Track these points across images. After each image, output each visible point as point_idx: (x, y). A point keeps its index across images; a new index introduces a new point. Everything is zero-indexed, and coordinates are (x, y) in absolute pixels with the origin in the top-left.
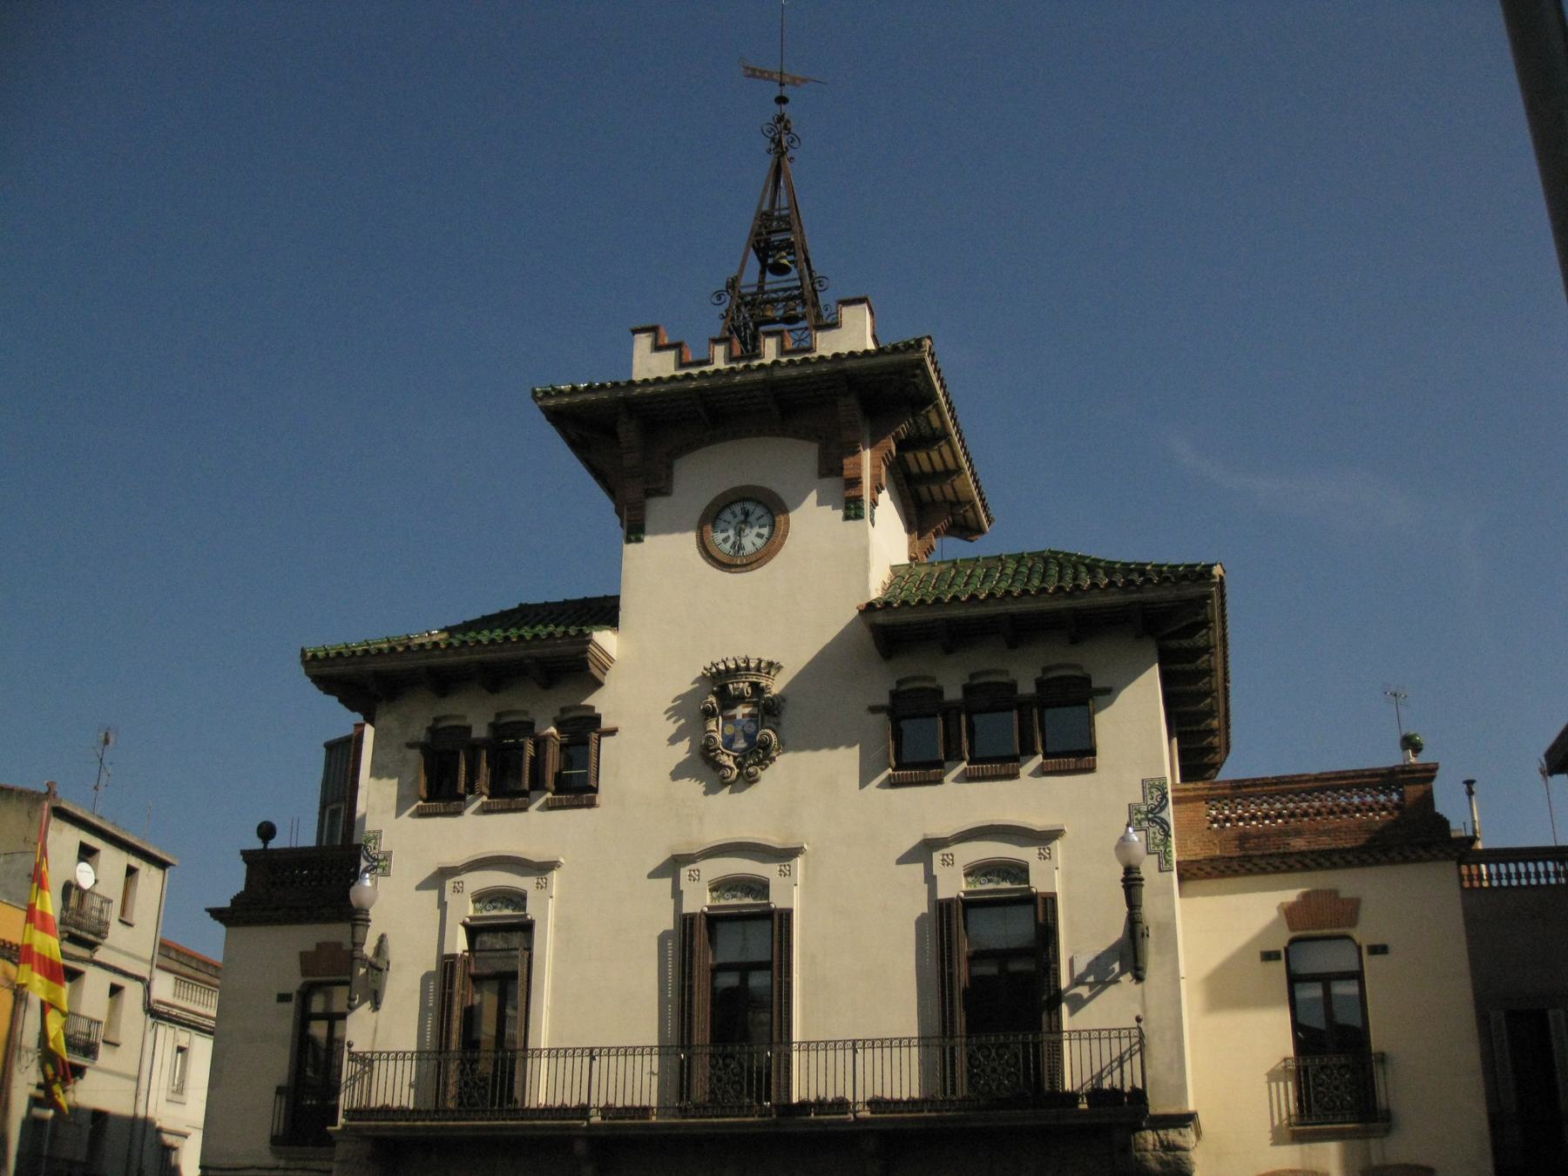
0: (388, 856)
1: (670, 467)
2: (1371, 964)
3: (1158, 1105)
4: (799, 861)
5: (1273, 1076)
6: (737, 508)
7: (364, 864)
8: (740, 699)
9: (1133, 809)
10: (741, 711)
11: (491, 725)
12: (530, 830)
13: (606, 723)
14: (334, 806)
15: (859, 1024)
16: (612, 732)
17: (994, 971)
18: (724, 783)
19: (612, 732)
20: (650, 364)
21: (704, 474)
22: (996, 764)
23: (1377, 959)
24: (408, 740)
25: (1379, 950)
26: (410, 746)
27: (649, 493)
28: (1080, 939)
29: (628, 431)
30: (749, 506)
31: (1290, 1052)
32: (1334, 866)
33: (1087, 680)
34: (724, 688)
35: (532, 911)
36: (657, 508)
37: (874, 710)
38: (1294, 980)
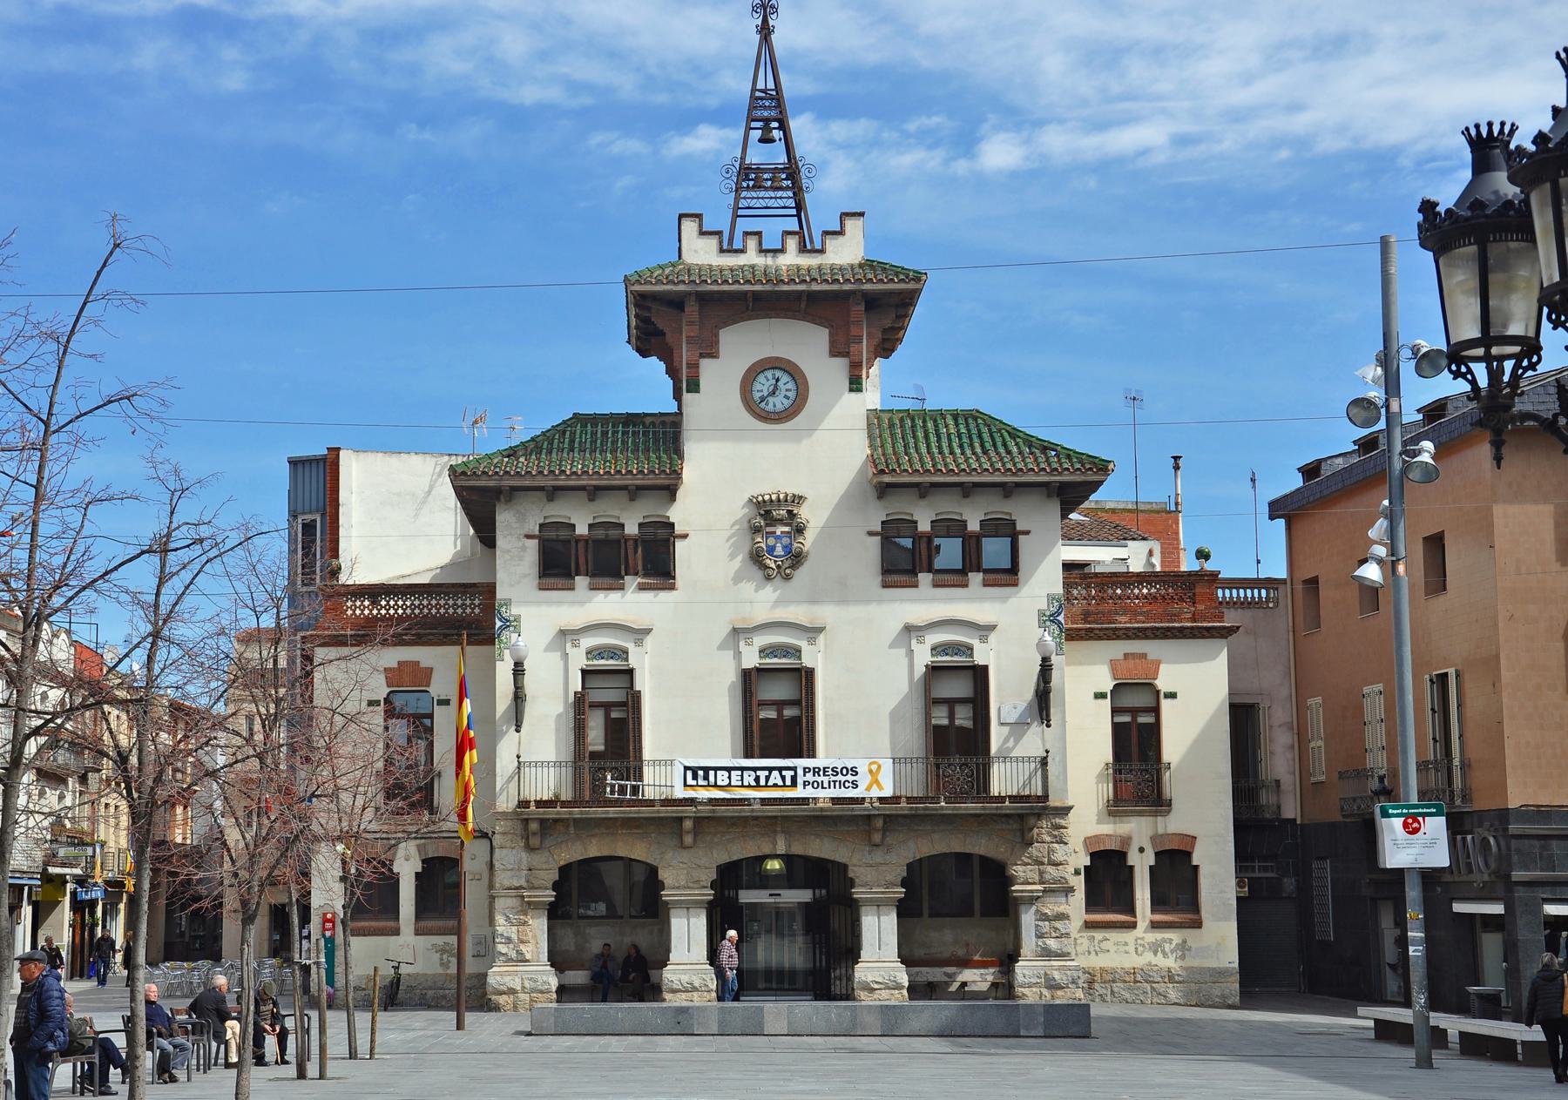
0: (517, 619)
1: (717, 336)
2: (1166, 705)
3: (1054, 801)
4: (822, 636)
5: (1100, 776)
6: (769, 374)
7: (498, 624)
8: (781, 521)
9: (1041, 613)
10: (780, 530)
11: (590, 526)
12: (627, 603)
13: (678, 530)
14: (309, 517)
15: (863, 748)
16: (685, 536)
17: (955, 718)
18: (768, 578)
19: (685, 536)
20: (701, 253)
21: (742, 345)
22: (954, 578)
23: (1169, 701)
24: (525, 531)
25: (1172, 696)
26: (528, 537)
27: (702, 356)
28: (1008, 696)
29: (692, 309)
30: (778, 373)
31: (1110, 759)
32: (1147, 638)
33: (1013, 523)
34: (768, 512)
35: (633, 662)
36: (708, 368)
37: (871, 534)
38: (1115, 711)
